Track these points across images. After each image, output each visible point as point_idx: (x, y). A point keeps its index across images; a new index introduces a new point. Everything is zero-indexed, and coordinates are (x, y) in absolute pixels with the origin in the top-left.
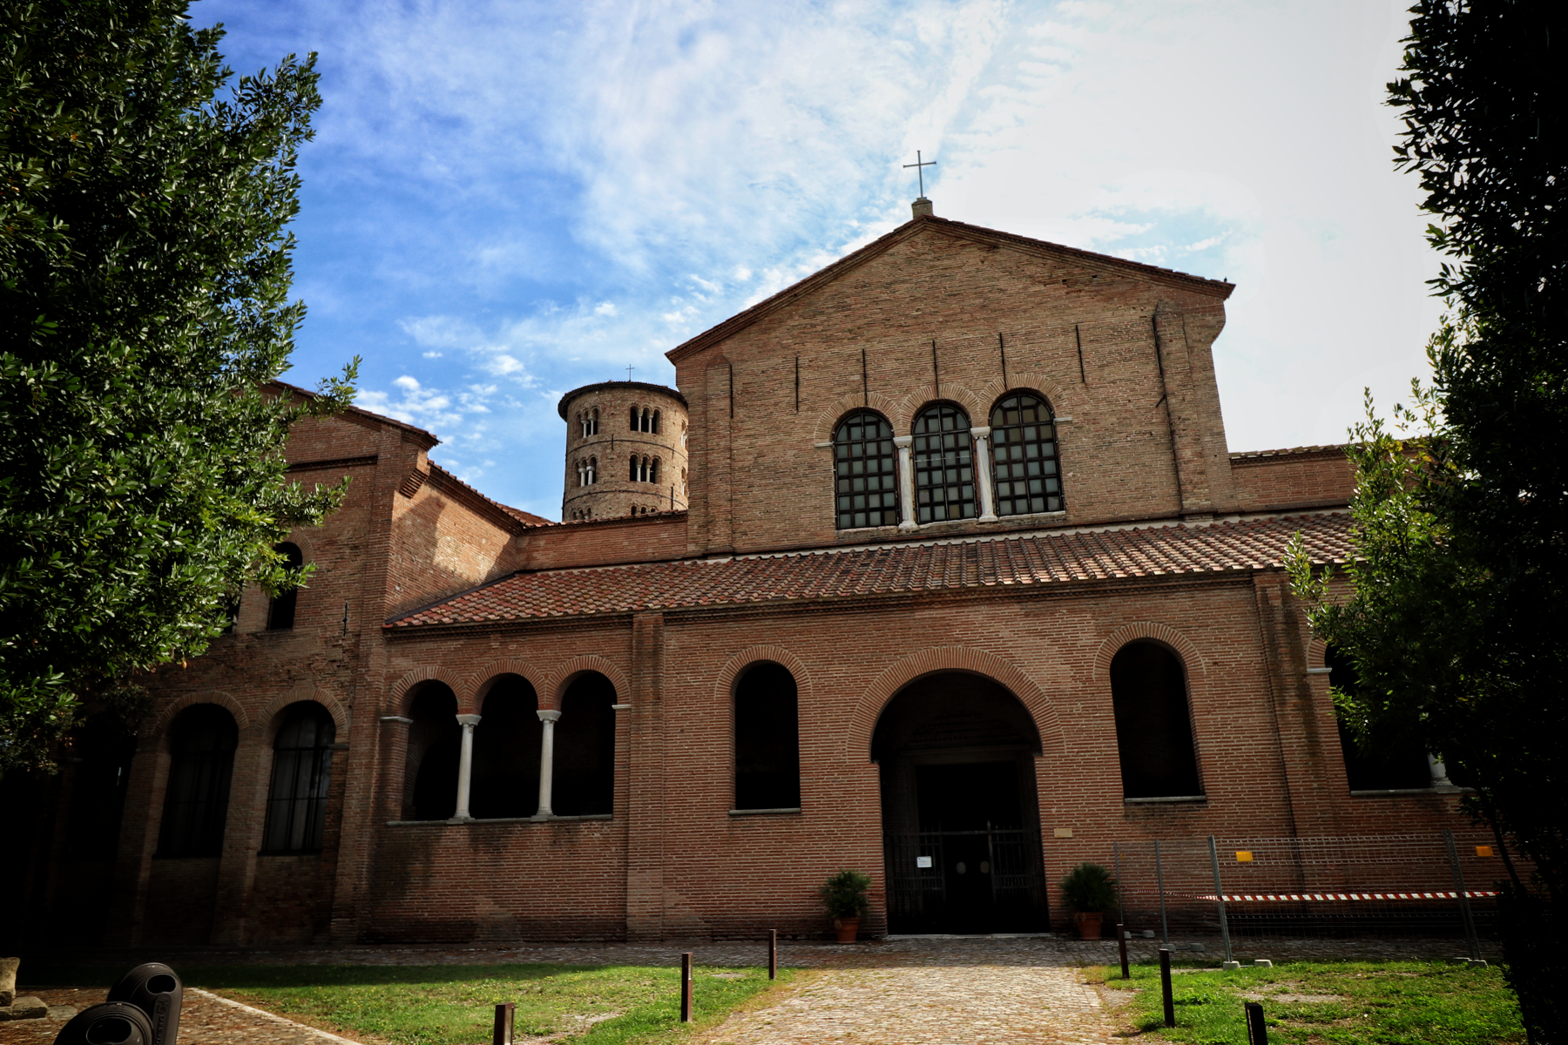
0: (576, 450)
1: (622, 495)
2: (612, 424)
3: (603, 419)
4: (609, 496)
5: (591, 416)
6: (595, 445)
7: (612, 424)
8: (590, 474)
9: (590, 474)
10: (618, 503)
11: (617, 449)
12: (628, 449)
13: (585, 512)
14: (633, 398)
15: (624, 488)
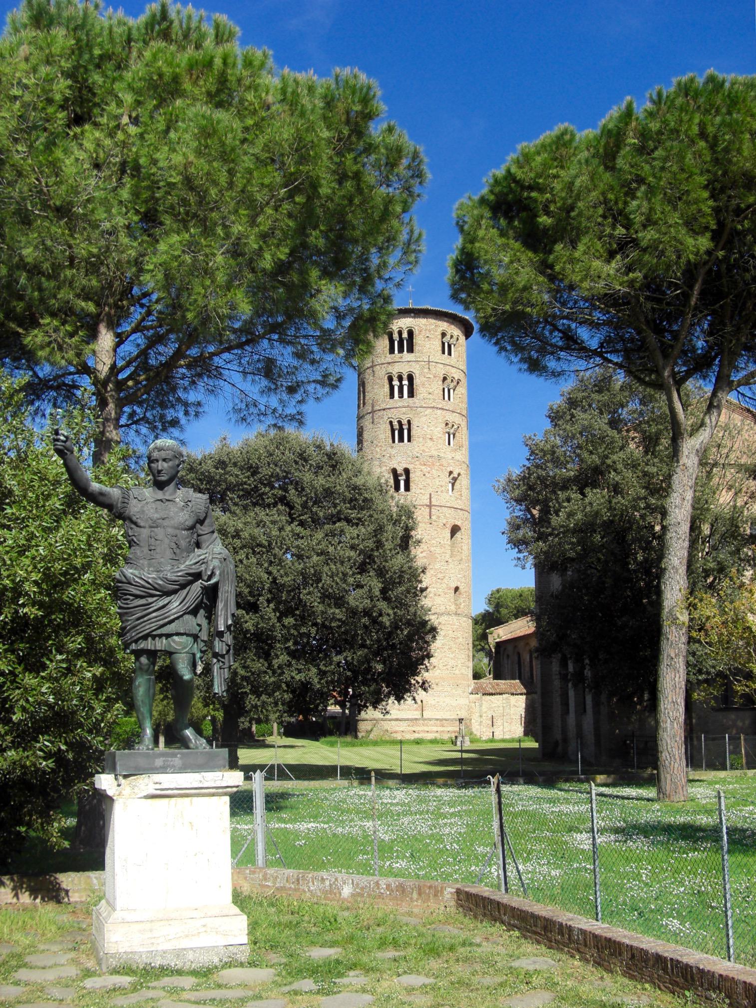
0: (389, 363)
1: (439, 412)
2: (428, 346)
3: (417, 340)
4: (429, 411)
5: (405, 335)
6: (413, 364)
7: (428, 346)
8: (405, 389)
9: (405, 389)
10: (436, 418)
11: (433, 370)
12: (441, 371)
13: (405, 422)
14: (443, 325)
15: (440, 406)
